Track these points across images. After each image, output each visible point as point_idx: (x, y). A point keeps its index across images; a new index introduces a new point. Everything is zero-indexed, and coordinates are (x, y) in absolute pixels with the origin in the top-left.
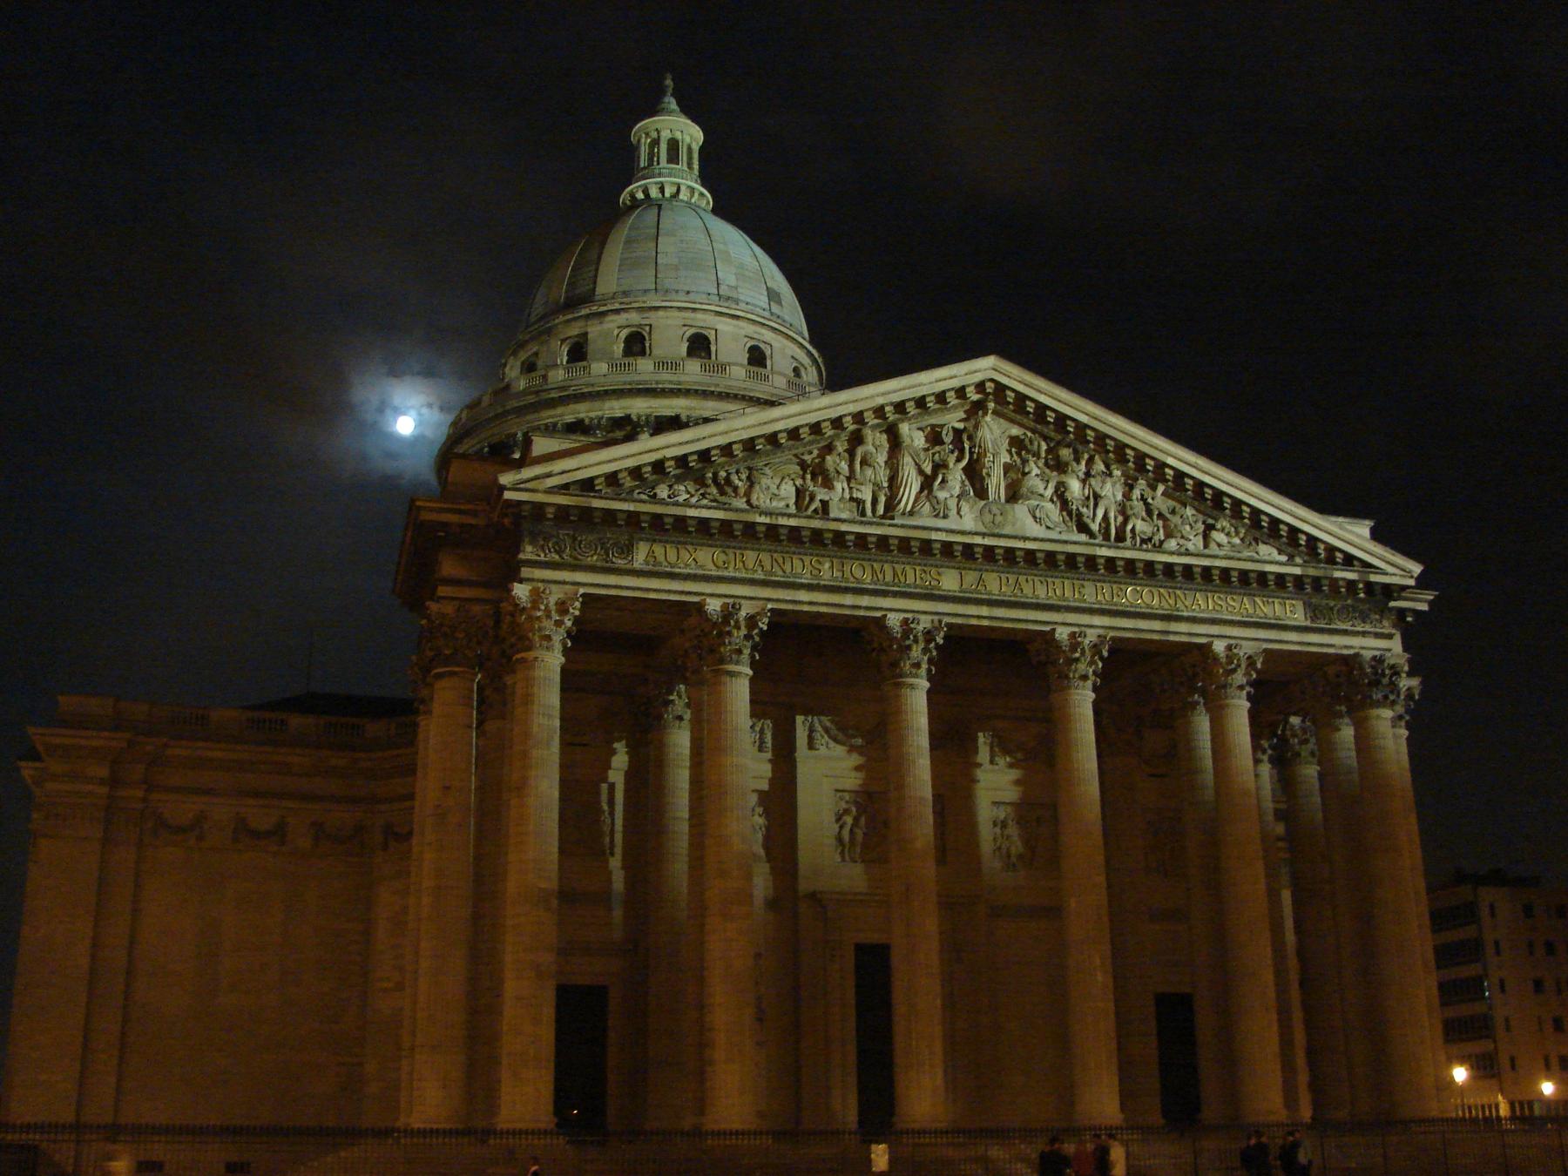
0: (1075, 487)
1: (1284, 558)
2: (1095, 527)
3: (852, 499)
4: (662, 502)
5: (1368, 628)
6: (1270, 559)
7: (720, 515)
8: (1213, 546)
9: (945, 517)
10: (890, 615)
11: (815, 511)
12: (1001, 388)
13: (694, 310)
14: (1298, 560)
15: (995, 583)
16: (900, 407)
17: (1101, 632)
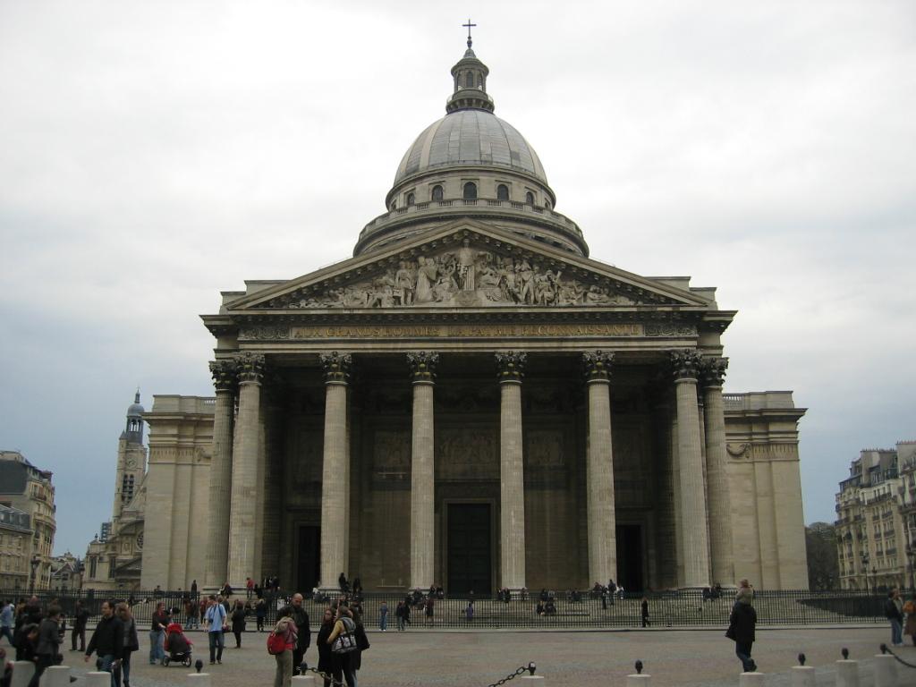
0: (511, 277)
1: (632, 303)
2: (522, 297)
3: (394, 297)
4: (303, 309)
5: (681, 335)
6: (624, 304)
7: (326, 312)
8: (589, 301)
9: (440, 301)
10: (411, 351)
11: (375, 305)
12: (472, 233)
13: (467, 171)
14: (640, 303)
15: (467, 332)
16: (417, 249)
17: (522, 350)
